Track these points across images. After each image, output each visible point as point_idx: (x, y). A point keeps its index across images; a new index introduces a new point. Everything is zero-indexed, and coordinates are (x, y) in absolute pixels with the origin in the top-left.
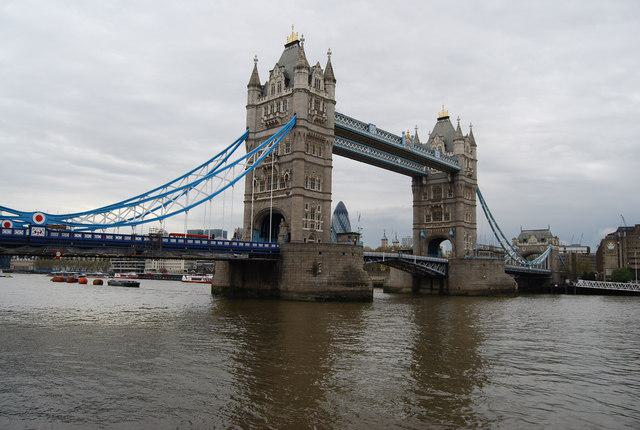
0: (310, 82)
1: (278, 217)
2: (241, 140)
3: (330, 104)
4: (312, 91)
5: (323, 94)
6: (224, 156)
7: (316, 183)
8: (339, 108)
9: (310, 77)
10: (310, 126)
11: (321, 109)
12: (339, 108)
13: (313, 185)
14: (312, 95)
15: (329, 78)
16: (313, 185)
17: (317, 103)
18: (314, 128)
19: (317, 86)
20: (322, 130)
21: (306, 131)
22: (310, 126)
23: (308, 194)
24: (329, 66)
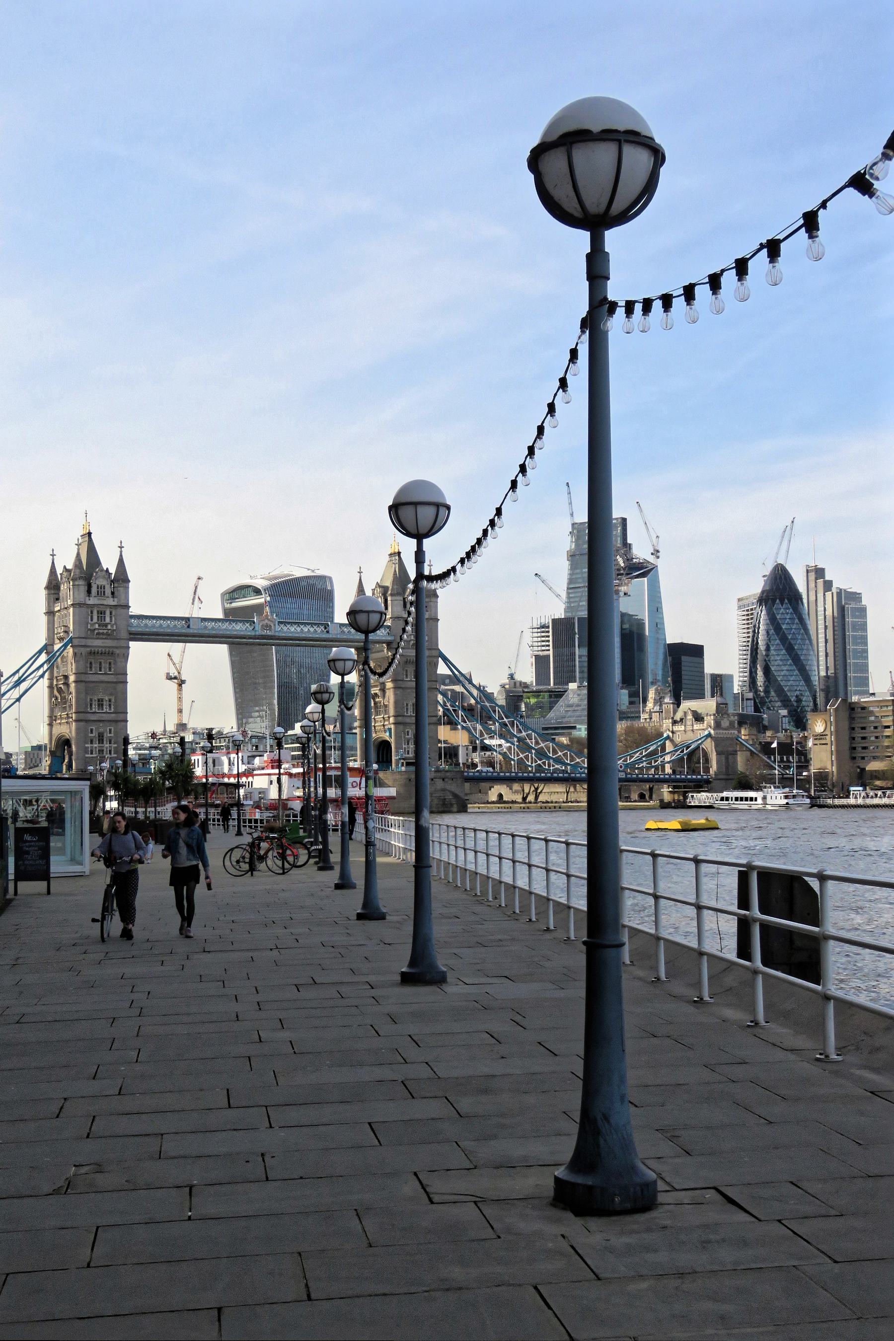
0: (89, 592)
1: (67, 742)
2: (40, 652)
3: (121, 611)
4: (92, 601)
5: (111, 602)
6: (16, 677)
7: (105, 703)
8: (134, 610)
9: (89, 586)
10: (90, 642)
11: (108, 620)
12: (134, 610)
13: (101, 705)
14: (92, 606)
15: (121, 579)
16: (101, 705)
17: (101, 613)
18: (98, 642)
19: (101, 592)
20: (109, 643)
21: (83, 650)
22: (90, 642)
23: (93, 717)
24: (121, 562)
